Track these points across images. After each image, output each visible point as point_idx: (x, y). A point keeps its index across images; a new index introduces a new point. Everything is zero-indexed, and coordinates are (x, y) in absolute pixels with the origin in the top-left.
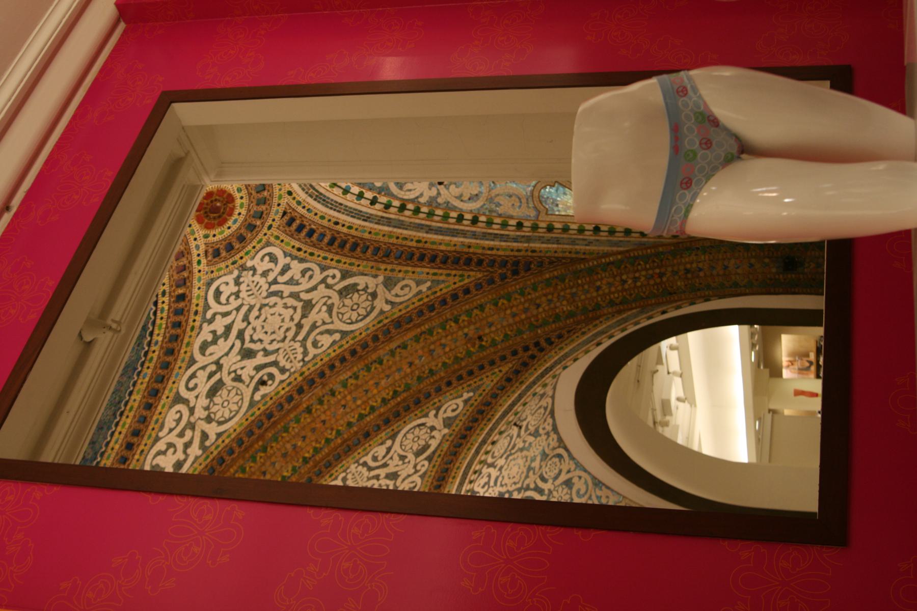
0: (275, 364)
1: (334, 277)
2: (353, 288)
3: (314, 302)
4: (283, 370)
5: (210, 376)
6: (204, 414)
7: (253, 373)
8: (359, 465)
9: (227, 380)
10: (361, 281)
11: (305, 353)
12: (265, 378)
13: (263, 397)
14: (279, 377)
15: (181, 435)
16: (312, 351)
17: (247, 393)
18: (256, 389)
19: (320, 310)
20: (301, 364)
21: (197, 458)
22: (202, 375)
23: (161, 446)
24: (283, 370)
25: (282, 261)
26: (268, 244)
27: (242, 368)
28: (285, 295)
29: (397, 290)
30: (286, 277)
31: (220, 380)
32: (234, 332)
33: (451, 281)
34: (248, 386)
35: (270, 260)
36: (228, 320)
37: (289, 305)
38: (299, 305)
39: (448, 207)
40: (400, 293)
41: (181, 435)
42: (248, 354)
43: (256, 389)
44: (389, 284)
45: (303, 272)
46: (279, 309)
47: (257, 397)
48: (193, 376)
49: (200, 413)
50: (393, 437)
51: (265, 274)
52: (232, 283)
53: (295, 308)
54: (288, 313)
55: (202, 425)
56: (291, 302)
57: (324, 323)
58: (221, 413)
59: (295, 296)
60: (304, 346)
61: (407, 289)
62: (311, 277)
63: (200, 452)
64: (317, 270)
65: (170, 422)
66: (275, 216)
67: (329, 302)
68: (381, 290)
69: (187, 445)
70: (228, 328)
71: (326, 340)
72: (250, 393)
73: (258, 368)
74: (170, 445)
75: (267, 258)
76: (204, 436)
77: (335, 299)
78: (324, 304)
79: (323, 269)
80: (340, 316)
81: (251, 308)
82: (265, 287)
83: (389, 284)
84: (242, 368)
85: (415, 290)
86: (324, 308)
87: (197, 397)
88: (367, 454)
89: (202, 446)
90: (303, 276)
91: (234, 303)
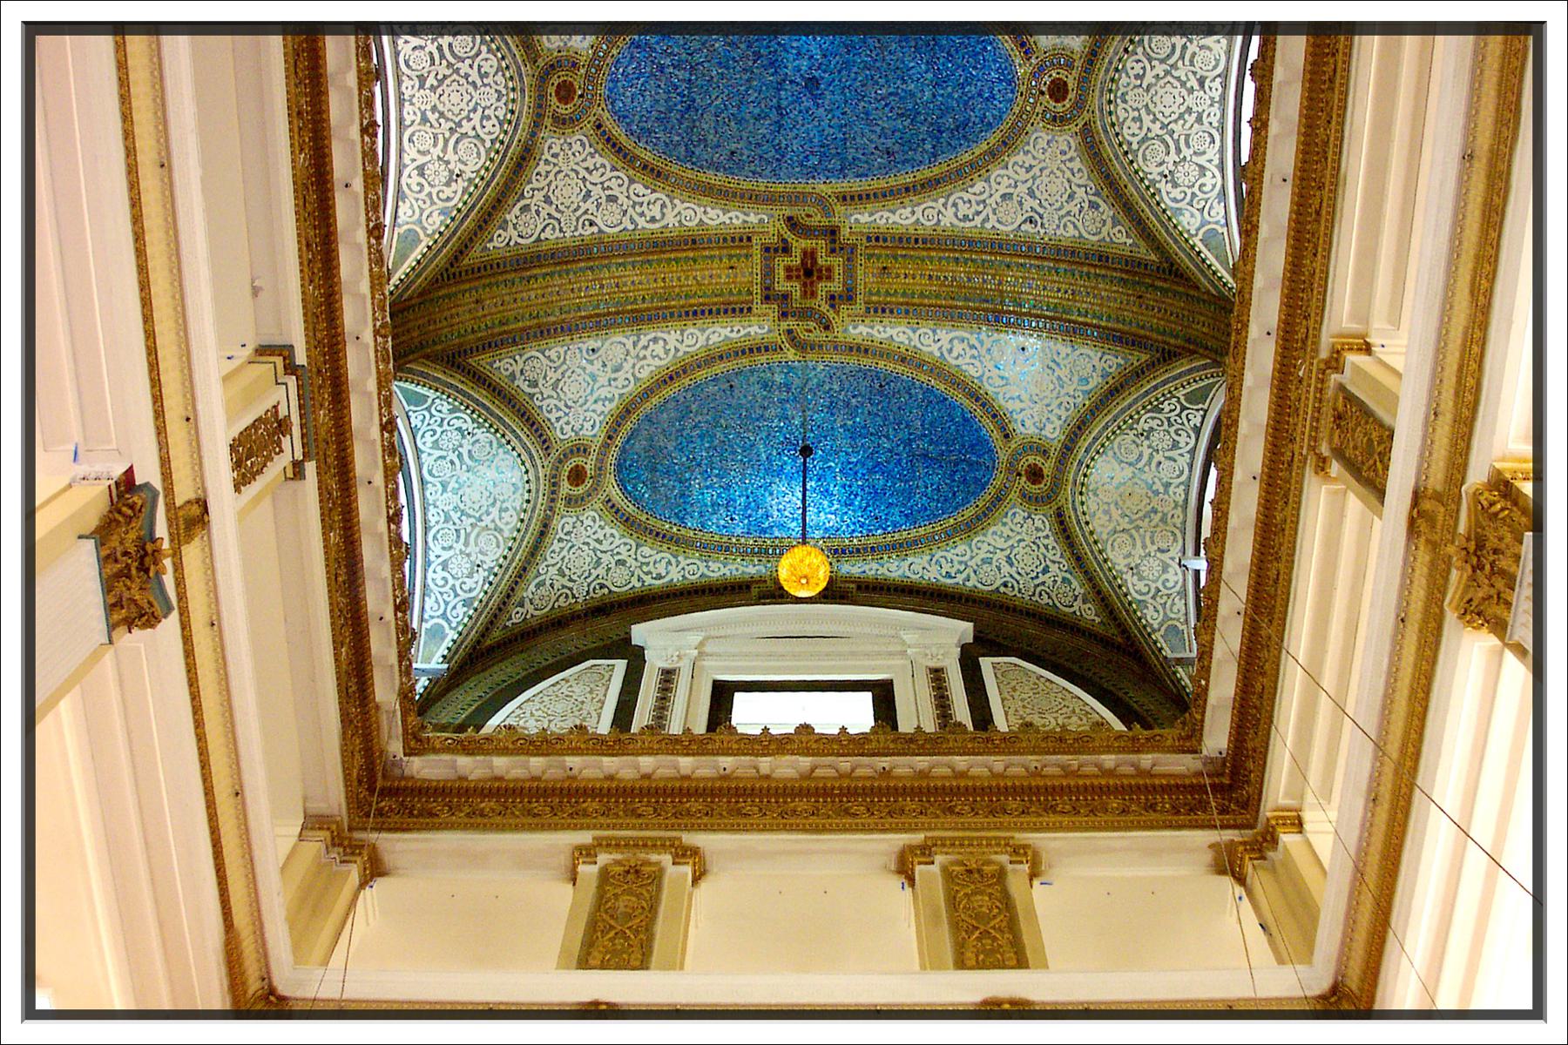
10: (525, 387)
14: (584, 347)
15: (645, 357)
16: (562, 351)
22: (620, 383)
23: (657, 362)
25: (558, 425)
30: (560, 414)
32: (595, 396)
33: (481, 361)
39: (473, 421)
41: (645, 357)
44: (513, 376)
45: (550, 412)
49: (631, 361)
50: (539, 240)
51: (568, 423)
55: (633, 352)
66: (554, 455)
68: (518, 374)
69: (645, 348)
71: (553, 354)
76: (635, 344)
91: (588, 414)
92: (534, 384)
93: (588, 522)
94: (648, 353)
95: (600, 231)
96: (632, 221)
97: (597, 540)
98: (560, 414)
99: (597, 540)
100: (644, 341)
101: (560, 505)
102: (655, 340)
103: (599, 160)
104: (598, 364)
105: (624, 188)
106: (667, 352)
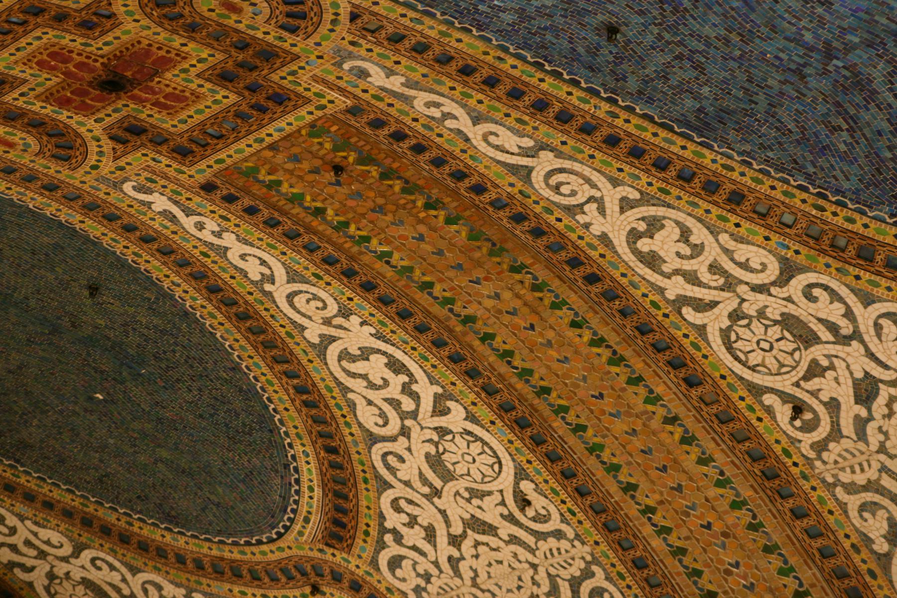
0: (836, 433)
4: (820, 447)
5: (833, 328)
6: (750, 309)
7: (825, 396)
8: (588, 563)
9: (817, 352)
11: (851, 488)
13: (769, 410)
14: (807, 439)
16: (853, 502)
17: (785, 384)
18: (785, 397)
20: (830, 480)
21: (661, 291)
23: (699, 234)
24: (820, 447)
27: (836, 380)
31: (817, 340)
34: (797, 384)
41: (714, 268)
42: (866, 391)
43: (785, 397)
47: (769, 399)
48: (835, 297)
49: (754, 303)
55: (729, 304)
58: (748, 337)
63: (671, 295)
65: (743, 252)
69: (692, 278)
72: (778, 386)
73: (833, 405)
74: (698, 250)
76: (702, 306)
84: (836, 380)
87: (789, 299)
88: (608, 578)
89: (683, 301)
94: (700, 266)
95: (520, 474)
96: (440, 410)
100: (676, 288)
102: (652, 260)
103: (393, 520)
104: (826, 386)
105: (399, 446)
106: (654, 225)
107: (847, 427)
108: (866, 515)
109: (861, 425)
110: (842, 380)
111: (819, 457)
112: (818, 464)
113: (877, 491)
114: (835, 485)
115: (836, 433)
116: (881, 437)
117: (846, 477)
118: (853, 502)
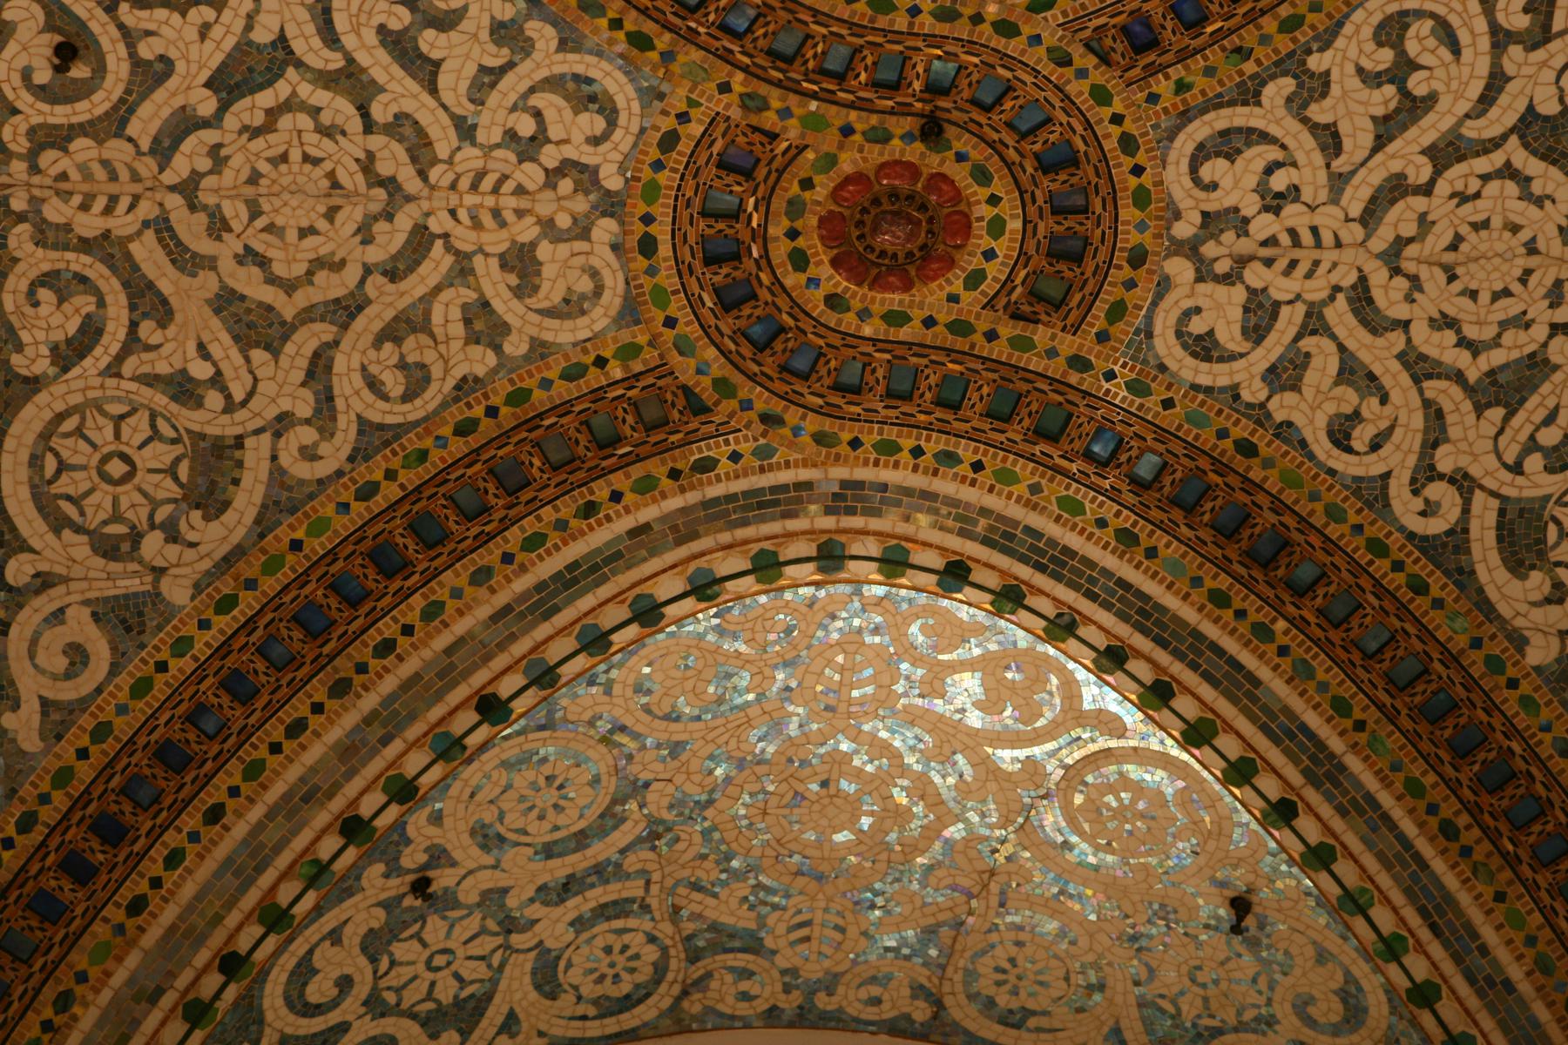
0: (116, 122)
1: (309, 454)
2: (211, 502)
3: (258, 355)
4: (59, 138)
7: (146, 51)
12: (79, 71)
16: (32, 259)
19: (203, 351)
20: (18, 204)
26: (630, 312)
27: (204, 31)
28: (376, 281)
29: (81, 627)
30: (447, 314)
32: (378, 64)
35: (582, 300)
36: (454, 82)
37: (321, 277)
38: (288, 309)
40: (54, 639)
46: (339, 237)
51: (522, 265)
52: (588, 156)
53: (289, 287)
54: (289, 261)
56: (330, 287)
57: (133, 343)
59: (347, 310)
60: (104, 246)
61: (61, 663)
62: (373, 384)
64: (379, 412)
67: (214, 400)
70: (427, 71)
71: (53, 321)
75: (585, 285)
77: (209, 419)
78: (217, 380)
79: (373, 437)
80: (116, 409)
81: (420, 151)
82: (465, 239)
83: (126, 618)
85: (29, 685)
86: (201, 370)
90: (402, 365)
91: (492, 122)
92: (212, 466)
93: (1236, 183)
97: (1386, 130)
98: (447, 314)
99: (1386, 130)
101: (1048, 347)
107: (147, 121)
108: (44, 294)
109: (185, 124)
110: (217, 32)
111: (32, 157)
112: (19, 168)
113: (108, 260)
114: (21, 218)
115: (116, 122)
116: (204, 164)
117: (55, 212)
118: (32, 259)
